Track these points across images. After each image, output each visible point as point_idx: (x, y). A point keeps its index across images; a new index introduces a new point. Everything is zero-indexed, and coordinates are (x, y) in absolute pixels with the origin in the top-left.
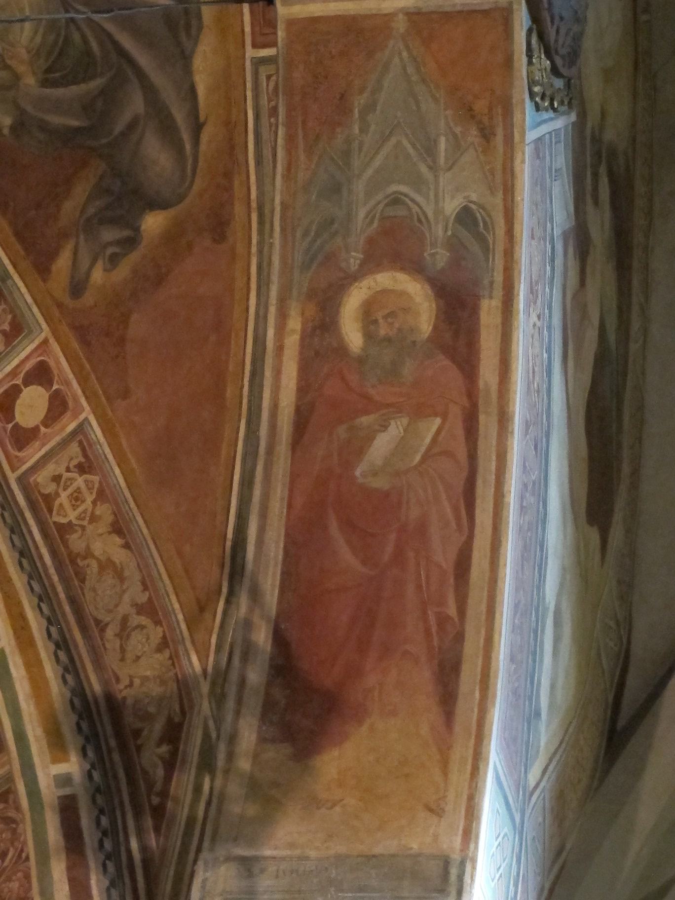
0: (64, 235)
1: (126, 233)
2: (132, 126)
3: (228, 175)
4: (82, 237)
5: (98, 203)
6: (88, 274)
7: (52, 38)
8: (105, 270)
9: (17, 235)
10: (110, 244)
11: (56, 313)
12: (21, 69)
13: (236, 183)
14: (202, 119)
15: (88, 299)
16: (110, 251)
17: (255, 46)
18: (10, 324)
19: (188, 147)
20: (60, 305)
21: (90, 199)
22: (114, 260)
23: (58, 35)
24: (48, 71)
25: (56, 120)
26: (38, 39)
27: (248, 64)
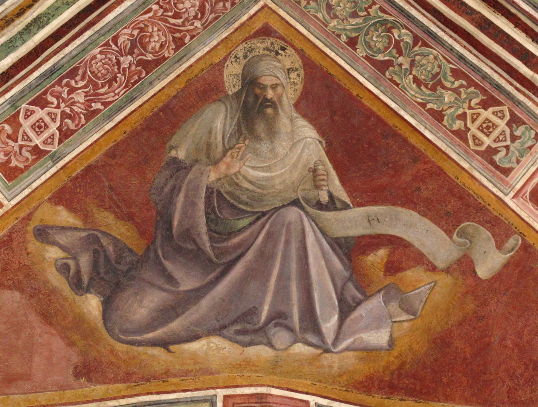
0: (86, 217)
1: (86, 279)
2: (171, 279)
3: (127, 378)
4: (84, 234)
5: (111, 249)
6: (54, 243)
7: (244, 198)
8: (56, 260)
9: (89, 169)
10: (78, 265)
11: (22, 214)
12: (222, 167)
13: (120, 386)
14: (172, 348)
15: (33, 245)
16: (71, 263)
17: (226, 397)
18: (16, 166)
19: (151, 335)
20: (29, 217)
21: (115, 241)
22: (64, 269)
23: (246, 204)
24: (219, 192)
25: (180, 199)
26: (246, 185)
27: (211, 392)
